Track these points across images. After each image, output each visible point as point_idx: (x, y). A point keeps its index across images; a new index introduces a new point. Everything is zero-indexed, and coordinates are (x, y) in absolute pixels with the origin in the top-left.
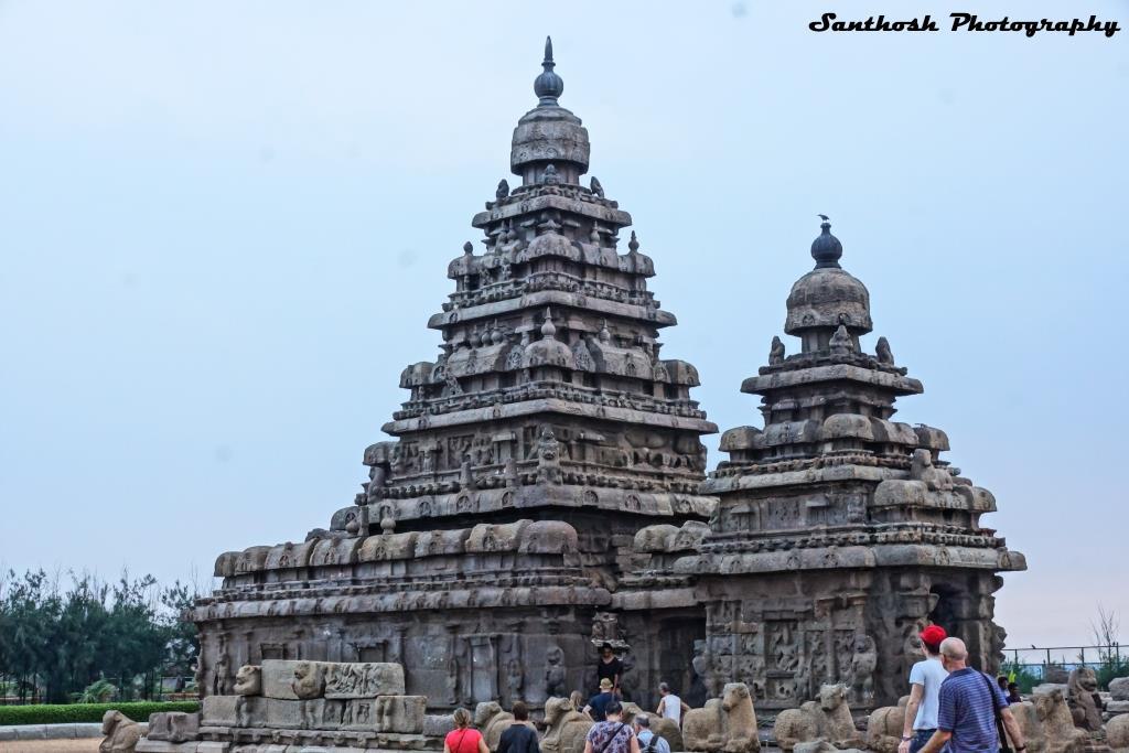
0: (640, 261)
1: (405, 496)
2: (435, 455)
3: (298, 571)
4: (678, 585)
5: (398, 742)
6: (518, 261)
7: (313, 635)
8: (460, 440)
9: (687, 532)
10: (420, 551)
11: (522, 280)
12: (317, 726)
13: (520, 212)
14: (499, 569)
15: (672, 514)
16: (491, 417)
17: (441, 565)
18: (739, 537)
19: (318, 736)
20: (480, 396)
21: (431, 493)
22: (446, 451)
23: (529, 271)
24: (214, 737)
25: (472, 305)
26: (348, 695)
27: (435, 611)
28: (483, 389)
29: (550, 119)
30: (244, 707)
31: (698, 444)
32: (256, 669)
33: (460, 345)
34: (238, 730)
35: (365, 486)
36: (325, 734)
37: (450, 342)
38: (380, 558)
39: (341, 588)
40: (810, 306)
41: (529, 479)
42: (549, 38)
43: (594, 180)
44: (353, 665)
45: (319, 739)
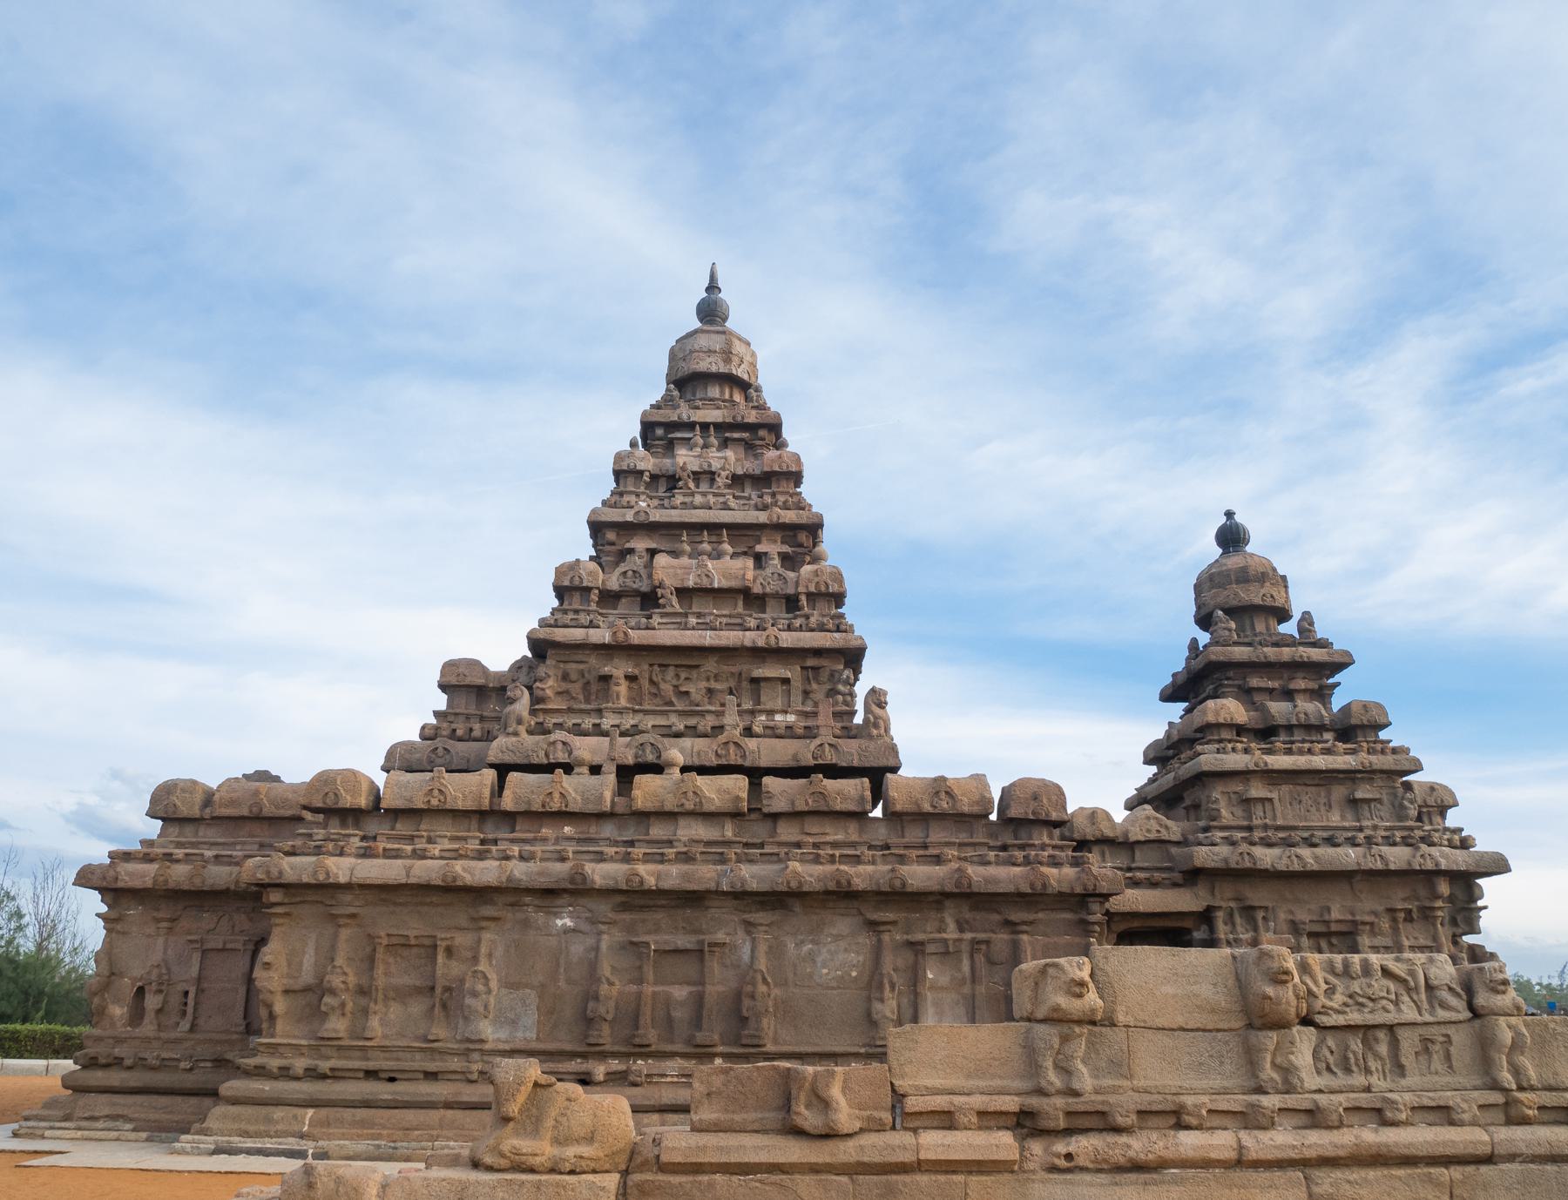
4: (1154, 885)
6: (740, 472)
7: (526, 924)
8: (672, 668)
17: (813, 826)
18: (1266, 827)
22: (645, 684)
34: (1059, 1102)
35: (437, 714)
37: (628, 545)
38: (689, 806)
40: (1268, 584)
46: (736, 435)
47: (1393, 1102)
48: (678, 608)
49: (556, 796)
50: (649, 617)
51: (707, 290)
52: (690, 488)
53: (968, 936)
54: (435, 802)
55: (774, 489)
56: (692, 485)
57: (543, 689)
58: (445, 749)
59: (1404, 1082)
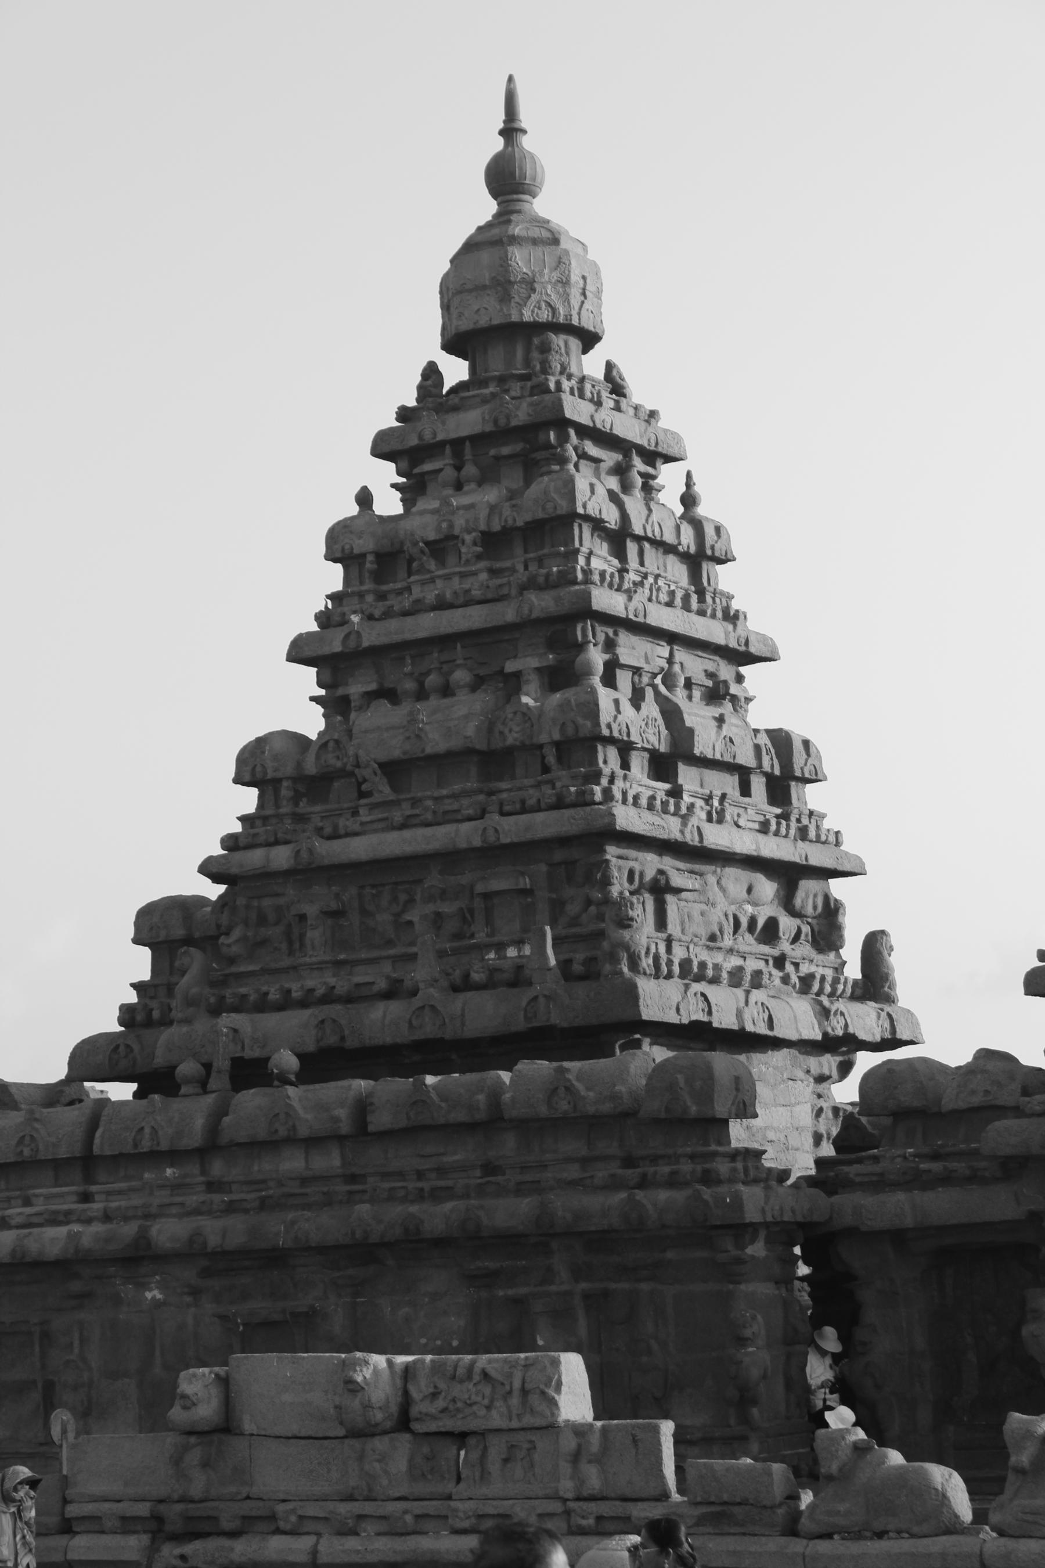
0: (709, 532)
1: (262, 1006)
2: (330, 922)
3: (58, 1166)
5: (628, 1519)
6: (496, 527)
9: (984, 1071)
10: (380, 1120)
11: (507, 564)
12: (397, 1495)
13: (489, 428)
14: (584, 1152)
15: (819, 1037)
16: (477, 842)
19: (406, 1512)
20: (437, 799)
21: (328, 998)
23: (519, 550)
24: (108, 1524)
25: (388, 614)
26: (473, 1425)
27: (440, 1243)
28: (439, 786)
29: (535, 242)
30: (194, 1456)
31: (827, 898)
32: (217, 1375)
33: (371, 697)
34: (179, 1507)
35: (138, 987)
36: (418, 1507)
37: (340, 692)
38: (283, 1132)
39: (193, 1200)
41: (577, 968)
42: (510, 79)
43: (609, 366)
44: (483, 1360)
45: (408, 1518)
46: (505, 451)
47: (456, 1510)
48: (392, 797)
49: (147, 1130)
50: (355, 813)
51: (502, 133)
52: (429, 571)
53: (584, 1285)
54: (27, 1152)
55: (546, 551)
56: (432, 565)
57: (229, 946)
58: (128, 1046)
59: (485, 1491)
